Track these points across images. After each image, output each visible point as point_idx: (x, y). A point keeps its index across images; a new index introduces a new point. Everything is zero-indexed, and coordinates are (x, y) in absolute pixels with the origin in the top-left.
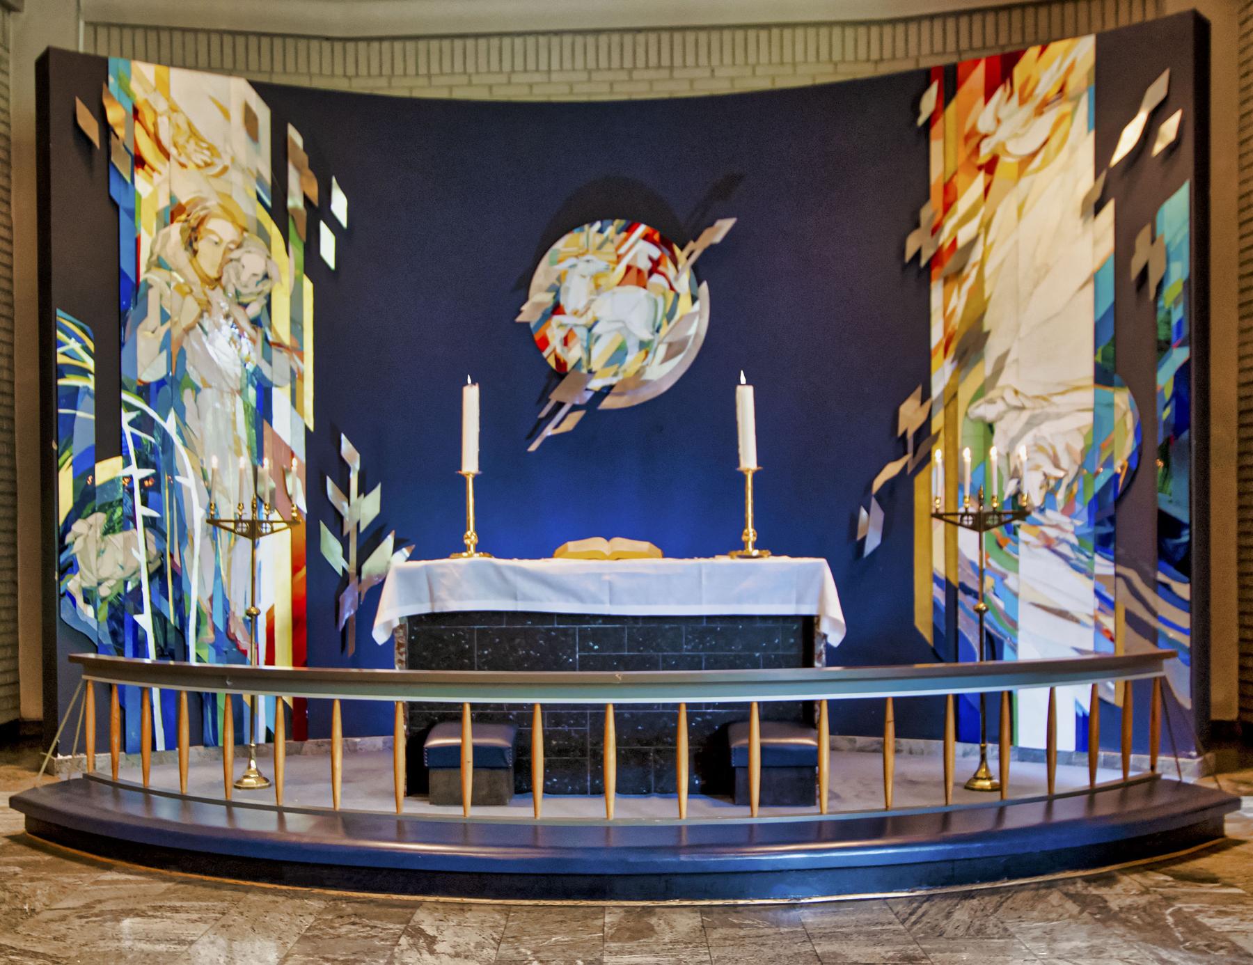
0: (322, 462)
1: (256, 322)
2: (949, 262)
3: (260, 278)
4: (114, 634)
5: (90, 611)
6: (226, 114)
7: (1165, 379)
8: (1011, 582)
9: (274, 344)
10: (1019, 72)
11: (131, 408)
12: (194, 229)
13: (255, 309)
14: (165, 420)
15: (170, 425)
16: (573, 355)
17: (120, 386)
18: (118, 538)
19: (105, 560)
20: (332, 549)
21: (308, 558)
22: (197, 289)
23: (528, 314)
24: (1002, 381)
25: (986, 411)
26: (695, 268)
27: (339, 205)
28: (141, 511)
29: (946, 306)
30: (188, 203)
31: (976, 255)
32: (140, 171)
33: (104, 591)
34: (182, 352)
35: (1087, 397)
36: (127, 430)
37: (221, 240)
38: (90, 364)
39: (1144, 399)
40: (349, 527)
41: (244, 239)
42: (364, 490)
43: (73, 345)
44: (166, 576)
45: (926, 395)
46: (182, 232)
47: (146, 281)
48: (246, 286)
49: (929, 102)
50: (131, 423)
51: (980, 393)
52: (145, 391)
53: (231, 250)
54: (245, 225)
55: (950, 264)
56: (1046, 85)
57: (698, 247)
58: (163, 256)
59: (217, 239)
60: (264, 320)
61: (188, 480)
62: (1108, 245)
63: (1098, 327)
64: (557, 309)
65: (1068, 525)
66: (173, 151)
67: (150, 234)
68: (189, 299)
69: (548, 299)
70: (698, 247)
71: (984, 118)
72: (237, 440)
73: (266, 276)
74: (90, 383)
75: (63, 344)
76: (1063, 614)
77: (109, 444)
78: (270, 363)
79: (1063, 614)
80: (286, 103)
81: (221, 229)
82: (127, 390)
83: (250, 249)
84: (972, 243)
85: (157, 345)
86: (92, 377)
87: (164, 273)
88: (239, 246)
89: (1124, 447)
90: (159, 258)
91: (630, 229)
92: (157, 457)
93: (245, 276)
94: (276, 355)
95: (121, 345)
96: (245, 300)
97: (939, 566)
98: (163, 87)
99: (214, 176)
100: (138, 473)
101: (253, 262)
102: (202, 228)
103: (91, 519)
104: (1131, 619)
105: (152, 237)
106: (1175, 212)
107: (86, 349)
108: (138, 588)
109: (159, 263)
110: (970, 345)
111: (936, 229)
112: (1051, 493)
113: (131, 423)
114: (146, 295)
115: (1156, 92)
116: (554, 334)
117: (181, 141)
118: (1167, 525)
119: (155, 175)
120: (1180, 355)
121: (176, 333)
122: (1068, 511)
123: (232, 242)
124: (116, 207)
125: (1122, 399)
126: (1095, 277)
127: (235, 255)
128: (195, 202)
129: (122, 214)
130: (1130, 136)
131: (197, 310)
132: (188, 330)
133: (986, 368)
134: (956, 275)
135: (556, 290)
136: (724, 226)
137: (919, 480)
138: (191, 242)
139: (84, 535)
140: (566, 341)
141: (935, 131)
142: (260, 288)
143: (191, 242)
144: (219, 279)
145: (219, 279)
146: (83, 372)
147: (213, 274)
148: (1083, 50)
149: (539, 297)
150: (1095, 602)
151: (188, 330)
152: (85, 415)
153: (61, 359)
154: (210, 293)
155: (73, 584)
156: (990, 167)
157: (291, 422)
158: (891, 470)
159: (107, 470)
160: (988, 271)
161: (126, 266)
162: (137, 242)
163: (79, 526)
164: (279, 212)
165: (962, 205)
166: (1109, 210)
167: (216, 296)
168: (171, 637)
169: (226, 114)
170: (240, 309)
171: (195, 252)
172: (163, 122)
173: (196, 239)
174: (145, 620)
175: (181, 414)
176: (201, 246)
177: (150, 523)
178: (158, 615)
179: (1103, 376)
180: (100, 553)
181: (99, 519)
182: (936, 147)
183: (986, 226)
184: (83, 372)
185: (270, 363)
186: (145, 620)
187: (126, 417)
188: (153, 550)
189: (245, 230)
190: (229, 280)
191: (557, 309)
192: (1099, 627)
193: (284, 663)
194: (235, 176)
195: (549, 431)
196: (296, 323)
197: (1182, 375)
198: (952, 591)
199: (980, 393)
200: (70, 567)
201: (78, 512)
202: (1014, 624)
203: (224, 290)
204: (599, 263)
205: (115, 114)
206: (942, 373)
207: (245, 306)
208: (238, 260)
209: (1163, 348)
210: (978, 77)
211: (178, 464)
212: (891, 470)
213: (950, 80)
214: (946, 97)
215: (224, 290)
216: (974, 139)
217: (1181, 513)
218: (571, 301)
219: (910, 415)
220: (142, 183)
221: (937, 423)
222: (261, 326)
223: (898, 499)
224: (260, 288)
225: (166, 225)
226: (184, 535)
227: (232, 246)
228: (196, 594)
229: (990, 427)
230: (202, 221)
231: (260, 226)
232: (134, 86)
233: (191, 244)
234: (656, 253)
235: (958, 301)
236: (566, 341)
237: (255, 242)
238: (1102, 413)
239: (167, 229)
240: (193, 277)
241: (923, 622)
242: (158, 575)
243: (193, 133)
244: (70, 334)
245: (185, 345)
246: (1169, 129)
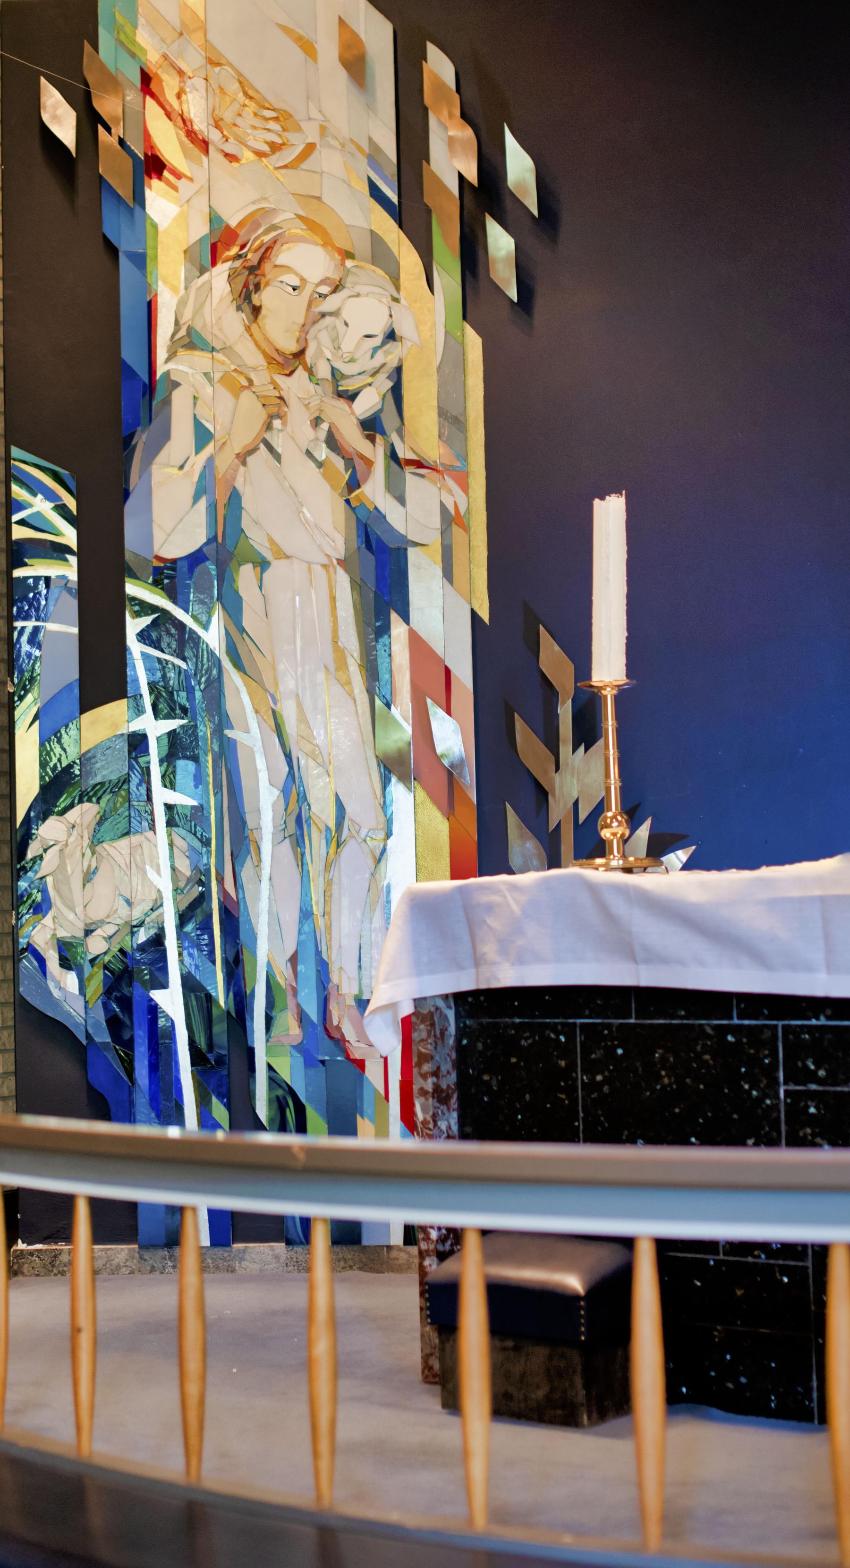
1: (371, 426)
3: (377, 341)
4: (114, 1024)
5: (71, 980)
6: (308, 48)
9: (410, 462)
11: (145, 608)
12: (253, 270)
13: (368, 402)
14: (206, 627)
15: (213, 636)
22: (261, 378)
28: (161, 795)
30: (241, 224)
32: (155, 182)
33: (96, 946)
34: (235, 498)
36: (135, 648)
37: (303, 280)
38: (69, 536)
41: (348, 272)
43: (41, 506)
44: (215, 917)
46: (232, 277)
47: (167, 374)
48: (352, 360)
50: (143, 636)
53: (323, 296)
54: (347, 247)
58: (198, 327)
59: (296, 282)
60: (389, 420)
61: (250, 735)
66: (214, 136)
67: (175, 289)
68: (247, 397)
72: (340, 654)
73: (391, 336)
75: (21, 507)
77: (101, 677)
78: (402, 500)
81: (304, 261)
82: (134, 576)
83: (358, 289)
85: (188, 489)
86: (73, 560)
87: (202, 359)
88: (337, 288)
90: (190, 330)
93: (350, 341)
96: (349, 386)
99: (285, 167)
100: (156, 729)
101: (364, 310)
102: (267, 267)
103: (73, 815)
105: (177, 291)
107: (62, 510)
108: (158, 941)
109: (190, 341)
113: (143, 636)
114: (167, 402)
117: (228, 116)
119: (181, 184)
121: (223, 464)
123: (323, 282)
124: (112, 251)
127: (328, 305)
128: (252, 221)
129: (123, 260)
131: (261, 415)
132: (242, 458)
142: (380, 358)
144: (300, 354)
145: (300, 354)
146: (59, 551)
147: (292, 347)
151: (242, 458)
152: (61, 627)
153: (19, 533)
154: (281, 380)
155: (41, 934)
161: (131, 353)
162: (150, 308)
163: (50, 830)
164: (409, 209)
167: (296, 386)
168: (220, 1029)
169: (308, 48)
170: (342, 404)
171: (256, 311)
173: (257, 287)
174: (170, 1001)
176: (265, 298)
180: (88, 877)
181: (85, 813)
184: (59, 551)
185: (402, 500)
186: (170, 1001)
187: (134, 625)
188: (185, 867)
189: (349, 255)
190: (319, 352)
194: (329, 161)
196: (451, 420)
203: (310, 371)
207: (351, 397)
208: (336, 314)
211: (230, 706)
215: (310, 371)
222: (383, 433)
224: (380, 358)
225: (202, 271)
227: (324, 290)
228: (268, 951)
230: (266, 252)
231: (375, 239)
233: (248, 298)
237: (368, 279)
239: (206, 276)
240: (252, 358)
244: (34, 487)
245: (239, 484)
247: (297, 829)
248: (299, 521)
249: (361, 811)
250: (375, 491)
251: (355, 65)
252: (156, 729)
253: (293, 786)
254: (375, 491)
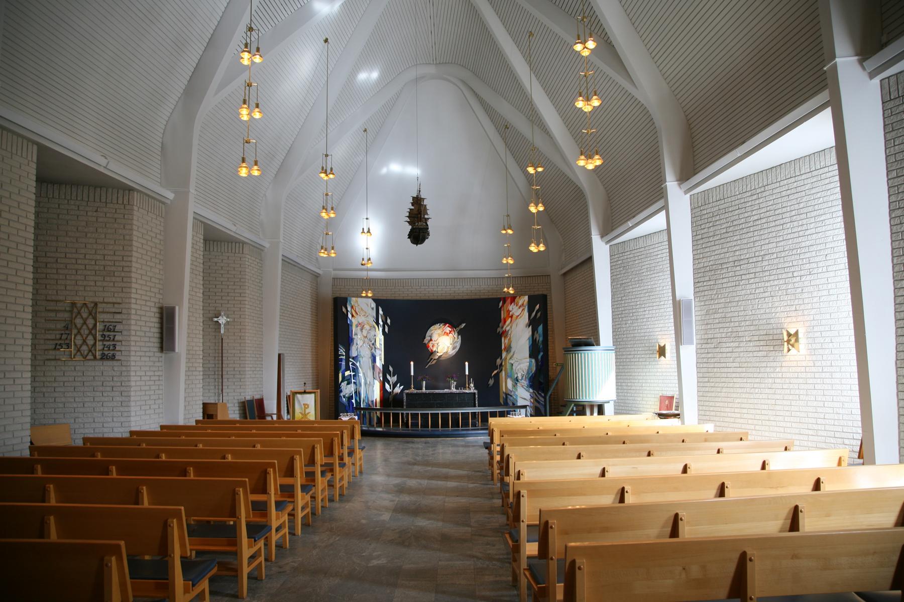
2: (505, 333)
7: (540, 357)
15: (358, 364)
23: (426, 341)
27: (389, 321)
29: (504, 342)
35: (528, 360)
39: (537, 361)
44: (357, 393)
52: (353, 358)
56: (520, 303)
65: (525, 383)
71: (510, 308)
77: (348, 368)
81: (367, 327)
89: (534, 369)
92: (355, 370)
100: (352, 374)
106: (540, 328)
110: (508, 349)
115: (538, 307)
116: (431, 345)
118: (540, 383)
125: (533, 361)
133: (512, 353)
134: (506, 337)
138: (362, 330)
139: (344, 385)
143: (362, 330)
149: (427, 338)
152: (344, 363)
156: (512, 317)
157: (380, 363)
159: (347, 373)
174: (354, 401)
179: (531, 356)
186: (354, 401)
193: (378, 407)
205: (349, 309)
206: (504, 354)
209: (539, 352)
210: (509, 300)
216: (509, 311)
218: (434, 339)
219: (498, 361)
235: (507, 341)
238: (530, 362)
241: (502, 401)
242: (356, 392)
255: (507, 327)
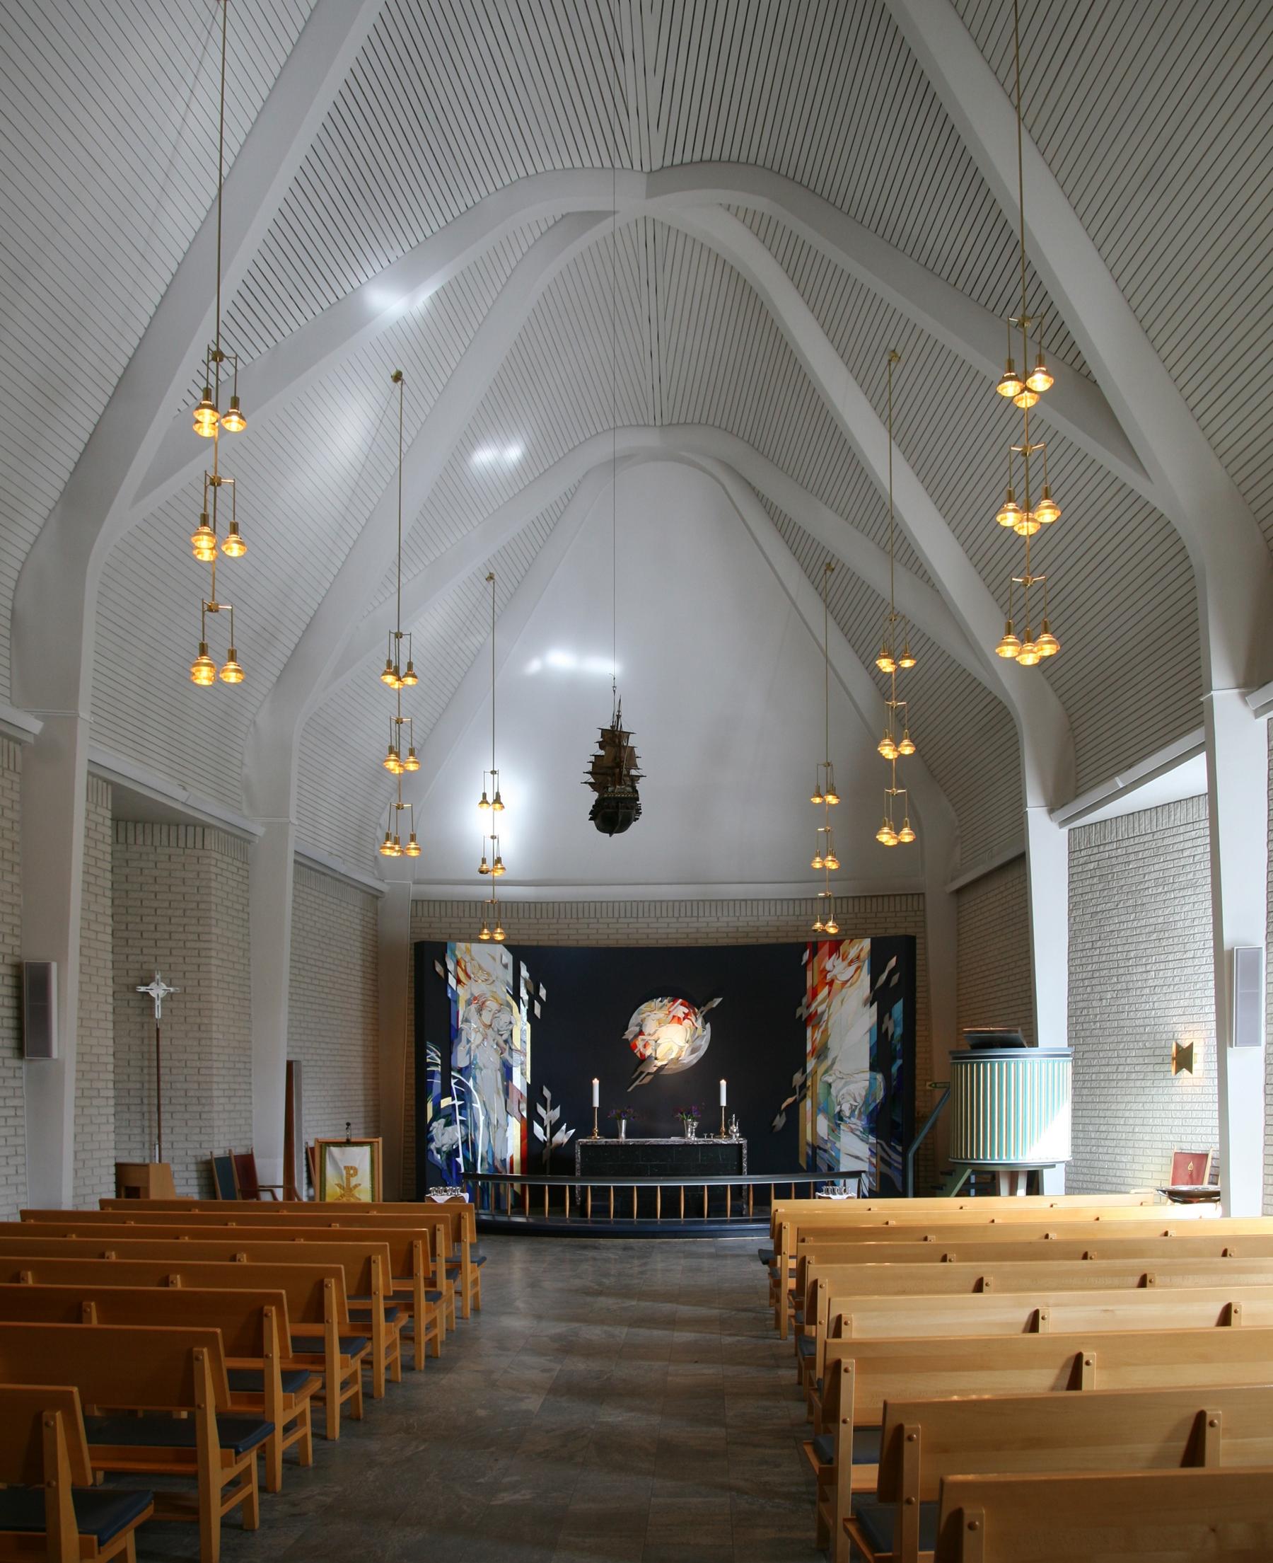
0: (534, 1095)
1: (506, 1041)
2: (814, 1019)
7: (894, 1069)
8: (838, 1145)
10: (842, 948)
13: (505, 1037)
15: (471, 1084)
16: (648, 1052)
17: (451, 1069)
18: (450, 1128)
19: (445, 1136)
20: (538, 1130)
21: (527, 1134)
23: (629, 1035)
24: (835, 1067)
25: (830, 1080)
26: (704, 1017)
27: (543, 993)
28: (459, 1118)
29: (812, 1037)
31: (825, 1017)
33: (444, 1149)
35: (867, 1075)
38: (439, 1061)
39: (887, 1078)
40: (546, 1122)
42: (553, 1108)
43: (433, 1054)
45: (804, 1071)
49: (806, 956)
51: (826, 1072)
52: (460, 1071)
55: (814, 1021)
56: (853, 953)
57: (705, 1009)
61: (478, 1105)
62: (875, 1018)
63: (871, 1049)
64: (641, 1033)
65: (859, 1123)
69: (637, 1029)
70: (705, 1009)
74: (439, 1069)
76: (857, 1157)
77: (447, 1092)
79: (857, 1157)
80: (519, 952)
81: (492, 1005)
84: (823, 1013)
89: (880, 1094)
91: (674, 1001)
92: (464, 1095)
93: (502, 1023)
94: (515, 1054)
95: (451, 1053)
97: (809, 1138)
98: (468, 951)
100: (457, 1103)
104: (882, 1159)
106: (898, 1008)
111: (809, 1006)
112: (853, 1112)
116: (640, 1044)
120: (899, 1062)
122: (859, 1118)
125: (879, 1077)
126: (870, 1030)
128: (480, 996)
130: (884, 977)
133: (829, 1062)
135: (640, 1025)
136: (718, 1001)
137: (801, 1105)
139: (437, 1126)
140: (645, 1046)
141: (809, 967)
146: (437, 1065)
148: (866, 944)
149: (632, 1029)
150: (868, 1153)
152: (437, 1081)
156: (831, 984)
157: (520, 1080)
158: (790, 1100)
159: (445, 1102)
160: (830, 1024)
161: (453, 1022)
163: (435, 1124)
164: (517, 997)
165: (821, 997)
166: (875, 1005)
167: (490, 1032)
172: (468, 965)
174: (460, 1160)
175: (475, 1079)
176: (484, 1012)
177: (462, 1122)
178: (465, 1158)
179: (873, 1068)
181: (442, 1121)
182: (809, 974)
183: (829, 1006)
184: (437, 1065)
186: (460, 1160)
187: (453, 1081)
191: (641, 1033)
192: (871, 1163)
193: (517, 1173)
195: (637, 1083)
197: (900, 1068)
198: (815, 1148)
199: (826, 1072)
200: (432, 1140)
201: (433, 1119)
202: (839, 1161)
204: (660, 1014)
205: (451, 966)
206: (811, 1064)
209: (894, 1060)
210: (826, 948)
212: (790, 1100)
213: (815, 948)
214: (814, 953)
216: (824, 972)
217: (898, 1119)
218: (647, 1030)
219: (798, 1078)
220: (460, 990)
221: (809, 1083)
223: (793, 1113)
226: (476, 1127)
229: (830, 1085)
232: (457, 953)
234: (686, 1011)
235: (818, 1035)
236: (645, 1046)
238: (872, 1081)
241: (803, 1162)
242: (465, 1142)
243: (480, 968)
246: (895, 979)
247: (488, 1124)
248: (488, 1060)
249: (502, 1122)
250: (506, 1055)
251: (506, 966)
252: (457, 1103)
253: (487, 1115)
254: (506, 1055)
255: (819, 1005)
